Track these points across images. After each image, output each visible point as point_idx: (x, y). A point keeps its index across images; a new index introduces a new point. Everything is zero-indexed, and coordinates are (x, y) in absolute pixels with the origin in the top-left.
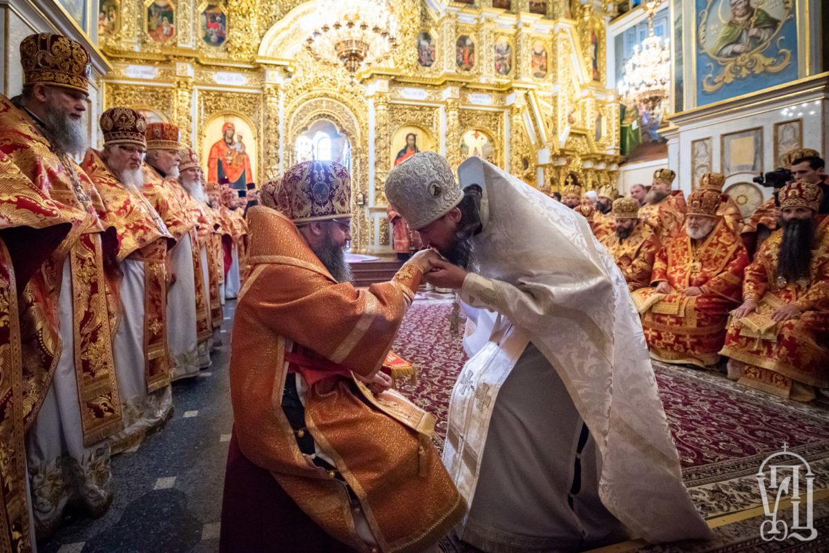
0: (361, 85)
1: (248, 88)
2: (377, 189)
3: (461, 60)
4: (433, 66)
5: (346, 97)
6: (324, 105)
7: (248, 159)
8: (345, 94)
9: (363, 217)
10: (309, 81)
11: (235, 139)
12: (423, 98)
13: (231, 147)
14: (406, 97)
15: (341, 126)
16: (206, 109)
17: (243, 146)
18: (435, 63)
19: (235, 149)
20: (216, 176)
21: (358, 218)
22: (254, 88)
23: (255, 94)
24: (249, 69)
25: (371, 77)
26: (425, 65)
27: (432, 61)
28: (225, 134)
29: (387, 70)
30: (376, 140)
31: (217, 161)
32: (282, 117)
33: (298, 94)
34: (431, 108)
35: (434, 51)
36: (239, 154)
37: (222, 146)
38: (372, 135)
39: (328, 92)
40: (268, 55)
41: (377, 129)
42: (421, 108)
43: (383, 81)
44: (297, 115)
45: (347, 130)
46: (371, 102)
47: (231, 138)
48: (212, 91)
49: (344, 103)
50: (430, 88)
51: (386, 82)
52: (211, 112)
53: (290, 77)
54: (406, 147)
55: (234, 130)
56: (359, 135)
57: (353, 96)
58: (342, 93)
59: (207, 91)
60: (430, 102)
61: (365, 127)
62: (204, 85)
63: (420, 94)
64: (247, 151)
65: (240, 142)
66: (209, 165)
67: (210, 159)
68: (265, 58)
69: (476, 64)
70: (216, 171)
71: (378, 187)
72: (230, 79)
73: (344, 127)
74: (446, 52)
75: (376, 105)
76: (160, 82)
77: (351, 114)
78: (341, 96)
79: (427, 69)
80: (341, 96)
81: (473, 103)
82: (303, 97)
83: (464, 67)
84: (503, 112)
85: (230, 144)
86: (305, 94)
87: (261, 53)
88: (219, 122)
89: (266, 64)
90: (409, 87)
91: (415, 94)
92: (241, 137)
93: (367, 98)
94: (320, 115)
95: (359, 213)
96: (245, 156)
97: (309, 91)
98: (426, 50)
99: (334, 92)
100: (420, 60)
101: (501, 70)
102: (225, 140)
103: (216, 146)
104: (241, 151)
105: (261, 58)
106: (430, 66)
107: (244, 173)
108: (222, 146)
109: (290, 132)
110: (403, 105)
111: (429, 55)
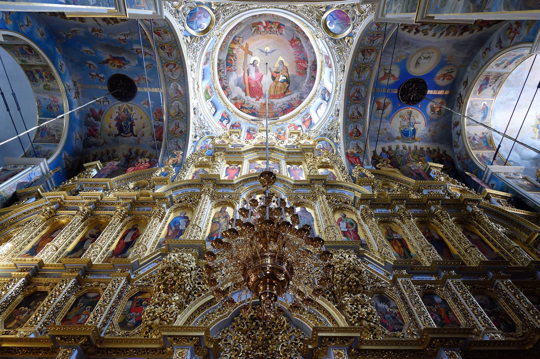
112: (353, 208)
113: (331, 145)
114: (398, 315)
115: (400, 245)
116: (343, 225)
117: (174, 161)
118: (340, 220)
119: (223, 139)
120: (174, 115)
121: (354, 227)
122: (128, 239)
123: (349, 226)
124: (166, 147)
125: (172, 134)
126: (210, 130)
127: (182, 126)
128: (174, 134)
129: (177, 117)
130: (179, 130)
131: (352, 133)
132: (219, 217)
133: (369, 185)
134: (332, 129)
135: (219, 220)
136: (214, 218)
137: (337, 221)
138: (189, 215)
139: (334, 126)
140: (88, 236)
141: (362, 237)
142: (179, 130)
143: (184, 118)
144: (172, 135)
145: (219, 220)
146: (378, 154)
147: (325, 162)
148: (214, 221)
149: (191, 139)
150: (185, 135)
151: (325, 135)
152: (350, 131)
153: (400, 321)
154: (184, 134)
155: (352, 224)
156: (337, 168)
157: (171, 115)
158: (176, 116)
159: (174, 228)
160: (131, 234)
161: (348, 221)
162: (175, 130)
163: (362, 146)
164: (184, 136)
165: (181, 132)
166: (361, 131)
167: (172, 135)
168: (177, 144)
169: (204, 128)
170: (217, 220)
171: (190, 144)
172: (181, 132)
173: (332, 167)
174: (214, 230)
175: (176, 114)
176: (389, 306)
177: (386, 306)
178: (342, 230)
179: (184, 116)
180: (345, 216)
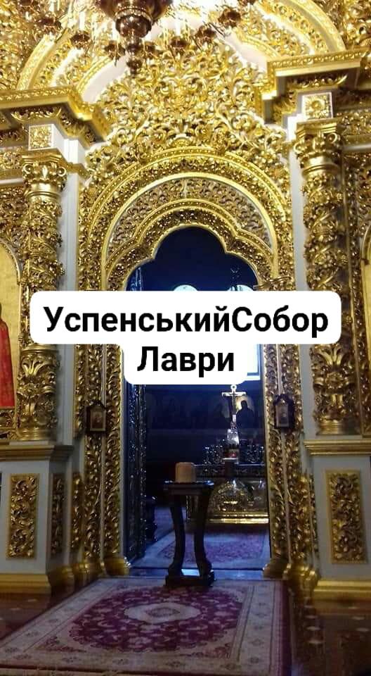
0: (271, 127)
2: (316, 386)
5: (233, 160)
6: (185, 189)
8: (233, 154)
15: (229, 234)
21: (283, 470)
25: (282, 99)
29: (316, 60)
30: (308, 249)
32: (70, 230)
38: (300, 236)
39: (189, 157)
41: (308, 222)
43: (314, 97)
44: (121, 221)
45: (245, 240)
53: (98, 139)
56: (274, 250)
57: (247, 153)
71: (320, 381)
73: (235, 233)
77: (253, 199)
78: (220, 159)
80: (220, 159)
86: (134, 172)
95: (285, 456)
97: (144, 162)
99: (204, 152)
109: (104, 263)
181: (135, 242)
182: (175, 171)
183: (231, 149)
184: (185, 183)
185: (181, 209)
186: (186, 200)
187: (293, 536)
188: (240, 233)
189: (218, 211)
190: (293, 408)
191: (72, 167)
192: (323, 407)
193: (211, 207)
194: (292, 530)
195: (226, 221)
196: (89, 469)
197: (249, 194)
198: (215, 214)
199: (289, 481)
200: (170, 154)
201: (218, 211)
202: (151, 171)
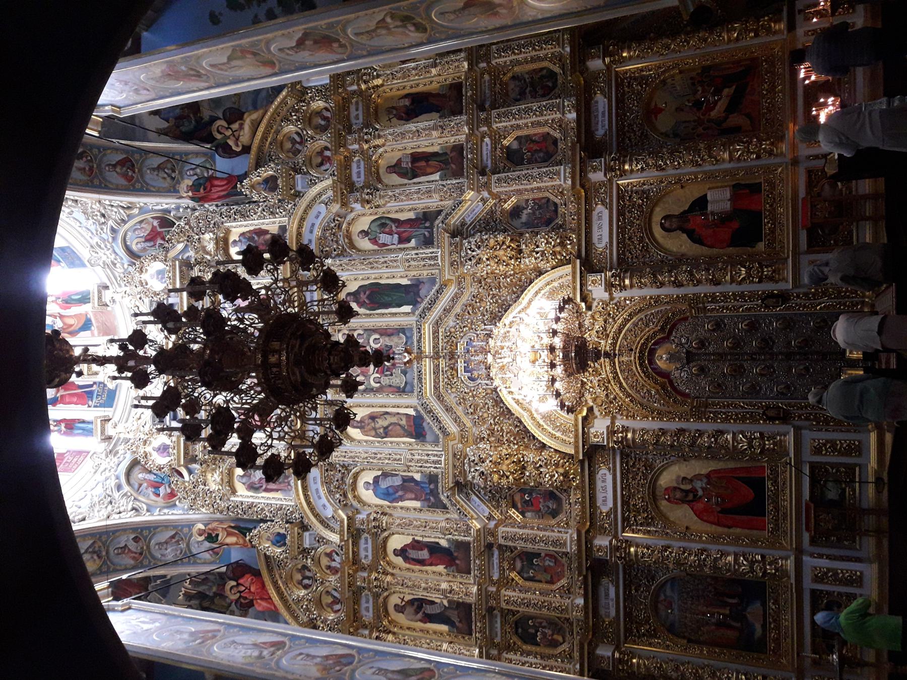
0: (594, 308)
1: (615, 466)
2: (760, 282)
3: (541, 155)
4: (556, 200)
5: (612, 329)
7: (715, 471)
9: (806, 294)
10: (595, 382)
11: (688, 487)
12: (606, 213)
13: (700, 493)
14: (606, 239)
16: (648, 525)
17: (698, 477)
18: (552, 197)
19: (702, 488)
20: (745, 518)
22: (614, 459)
23: (622, 459)
24: (589, 465)
26: (556, 211)
27: (549, 200)
28: (683, 501)
31: (720, 515)
33: (615, 398)
34: (619, 197)
35: (534, 200)
36: (708, 483)
37: (700, 506)
40: (572, 440)
42: (620, 213)
46: (617, 295)
47: (687, 492)
48: (623, 514)
49: (620, 333)
50: (591, 206)
51: (591, 278)
52: (652, 518)
54: (684, 231)
55: (675, 488)
58: (608, 336)
59: (624, 519)
60: (611, 200)
61: (657, 300)
62: (616, 524)
63: (600, 218)
64: (704, 472)
65: (691, 481)
66: (729, 527)
67: (718, 524)
68: (576, 448)
69: (546, 129)
70: (738, 517)
72: (604, 489)
73: (656, 329)
74: (535, 185)
75: (624, 288)
76: (618, 578)
78: (611, 335)
79: (561, 210)
81: (607, 127)
82: (617, 389)
83: (551, 148)
84: (617, 72)
85: (695, 496)
87: (571, 450)
88: (664, 504)
89: (583, 446)
90: (591, 238)
91: (600, 228)
92: (684, 478)
93: (612, 299)
94: (641, 365)
96: (712, 476)
97: (609, 382)
98: (534, 213)
100: (548, 222)
101: (550, 84)
102: (689, 502)
103: (699, 514)
104: (705, 480)
105: (577, 452)
106: (555, 205)
107: (738, 478)
108: (700, 506)
110: (618, 243)
111: (540, 207)
112: (352, 216)
113: (141, 222)
114: (537, 201)
115: (423, 163)
116: (384, 238)
117: (229, 534)
118: (374, 241)
119: (149, 449)
120: (98, 561)
121: (388, 222)
122: (424, 554)
123: (387, 230)
124: (175, 563)
125: (142, 558)
126: (112, 482)
127: (126, 540)
128: (141, 554)
129: (104, 553)
130: (132, 546)
131: (125, 176)
132: (375, 429)
133: (293, 178)
134: (103, 216)
135: (380, 428)
136: (377, 435)
137: (376, 247)
138: (368, 477)
139: (99, 211)
140: (420, 615)
141: (411, 215)
142: (132, 546)
143: (104, 538)
144: (145, 557)
145: (380, 428)
146: (165, 125)
147: (217, 243)
148: (383, 435)
149: (145, 517)
150: (142, 532)
151: (113, 230)
152: (122, 182)
153: (543, 201)
154: (141, 533)
155: (383, 225)
156: (234, 224)
157: (100, 568)
158: (99, 557)
159: (400, 493)
160: (413, 554)
161: (375, 227)
162: (132, 552)
163: (156, 161)
164: (145, 533)
165: (136, 540)
166: (120, 157)
167: (145, 557)
168: (166, 543)
169: (109, 496)
170: (382, 430)
171: (157, 516)
172: (136, 540)
173: (228, 232)
174: (402, 432)
175: (95, 557)
176: (524, 208)
177: (525, 212)
178: (396, 242)
179: (100, 539)
180: (365, 233)
181: (658, 390)
182: (614, 363)
183: (605, 330)
184: (622, 359)
185: (637, 362)
186: (632, 358)
187: (848, 297)
188: (657, 326)
189: (641, 339)
190: (771, 295)
191: (613, 423)
192: (771, 279)
193: (638, 343)
194: (845, 298)
195: (647, 334)
196: (807, 419)
197: (632, 321)
198: (642, 341)
199: (815, 299)
200: (605, 366)
201: (641, 339)
202: (614, 378)
